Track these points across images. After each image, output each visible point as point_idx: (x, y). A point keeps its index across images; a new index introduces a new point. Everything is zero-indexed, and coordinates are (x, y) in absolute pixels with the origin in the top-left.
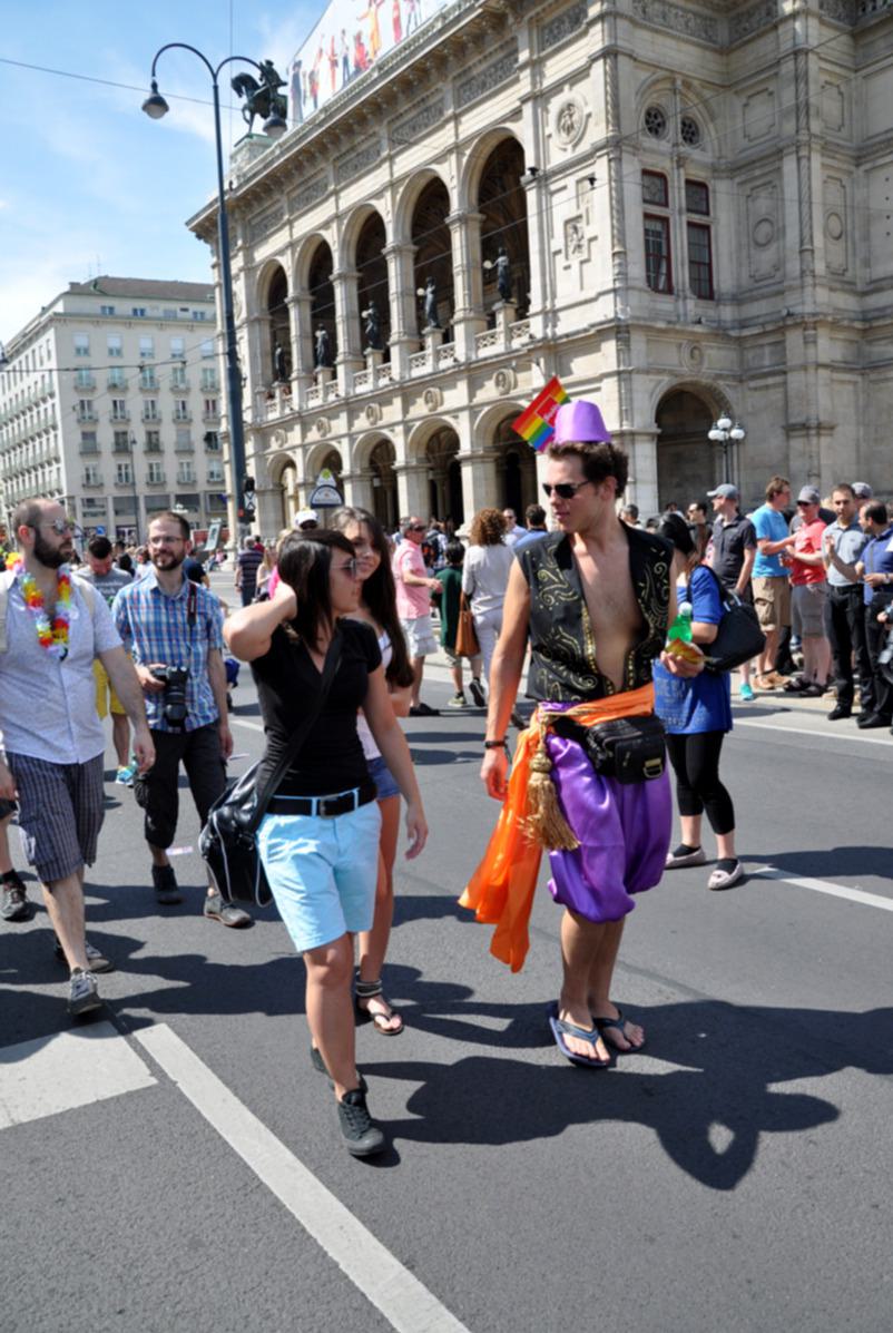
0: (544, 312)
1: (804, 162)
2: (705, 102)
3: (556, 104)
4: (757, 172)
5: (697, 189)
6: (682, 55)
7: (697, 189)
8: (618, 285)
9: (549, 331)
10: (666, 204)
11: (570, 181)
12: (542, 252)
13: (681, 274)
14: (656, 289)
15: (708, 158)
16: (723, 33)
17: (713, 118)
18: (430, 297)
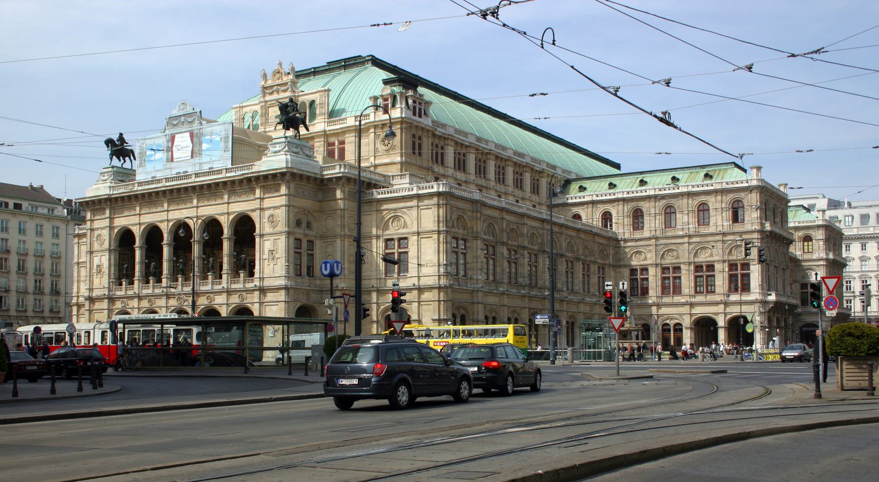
0: (260, 278)
1: (343, 241)
2: (313, 216)
3: (267, 213)
4: (329, 240)
5: (310, 242)
6: (307, 204)
7: (310, 242)
8: (286, 275)
9: (261, 284)
10: (301, 249)
11: (272, 238)
12: (260, 260)
13: (304, 270)
14: (297, 275)
15: (314, 233)
16: (320, 196)
17: (316, 221)
18: (211, 262)
